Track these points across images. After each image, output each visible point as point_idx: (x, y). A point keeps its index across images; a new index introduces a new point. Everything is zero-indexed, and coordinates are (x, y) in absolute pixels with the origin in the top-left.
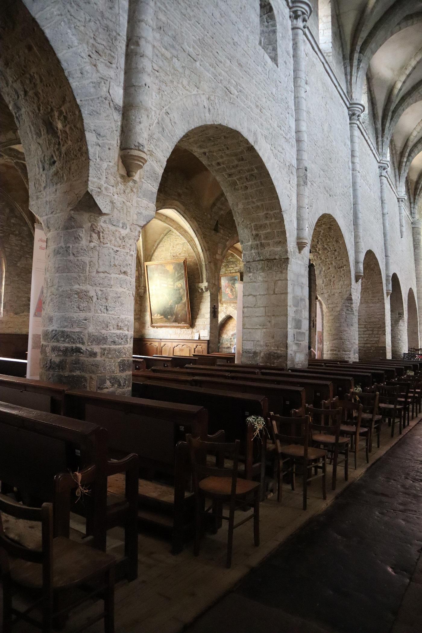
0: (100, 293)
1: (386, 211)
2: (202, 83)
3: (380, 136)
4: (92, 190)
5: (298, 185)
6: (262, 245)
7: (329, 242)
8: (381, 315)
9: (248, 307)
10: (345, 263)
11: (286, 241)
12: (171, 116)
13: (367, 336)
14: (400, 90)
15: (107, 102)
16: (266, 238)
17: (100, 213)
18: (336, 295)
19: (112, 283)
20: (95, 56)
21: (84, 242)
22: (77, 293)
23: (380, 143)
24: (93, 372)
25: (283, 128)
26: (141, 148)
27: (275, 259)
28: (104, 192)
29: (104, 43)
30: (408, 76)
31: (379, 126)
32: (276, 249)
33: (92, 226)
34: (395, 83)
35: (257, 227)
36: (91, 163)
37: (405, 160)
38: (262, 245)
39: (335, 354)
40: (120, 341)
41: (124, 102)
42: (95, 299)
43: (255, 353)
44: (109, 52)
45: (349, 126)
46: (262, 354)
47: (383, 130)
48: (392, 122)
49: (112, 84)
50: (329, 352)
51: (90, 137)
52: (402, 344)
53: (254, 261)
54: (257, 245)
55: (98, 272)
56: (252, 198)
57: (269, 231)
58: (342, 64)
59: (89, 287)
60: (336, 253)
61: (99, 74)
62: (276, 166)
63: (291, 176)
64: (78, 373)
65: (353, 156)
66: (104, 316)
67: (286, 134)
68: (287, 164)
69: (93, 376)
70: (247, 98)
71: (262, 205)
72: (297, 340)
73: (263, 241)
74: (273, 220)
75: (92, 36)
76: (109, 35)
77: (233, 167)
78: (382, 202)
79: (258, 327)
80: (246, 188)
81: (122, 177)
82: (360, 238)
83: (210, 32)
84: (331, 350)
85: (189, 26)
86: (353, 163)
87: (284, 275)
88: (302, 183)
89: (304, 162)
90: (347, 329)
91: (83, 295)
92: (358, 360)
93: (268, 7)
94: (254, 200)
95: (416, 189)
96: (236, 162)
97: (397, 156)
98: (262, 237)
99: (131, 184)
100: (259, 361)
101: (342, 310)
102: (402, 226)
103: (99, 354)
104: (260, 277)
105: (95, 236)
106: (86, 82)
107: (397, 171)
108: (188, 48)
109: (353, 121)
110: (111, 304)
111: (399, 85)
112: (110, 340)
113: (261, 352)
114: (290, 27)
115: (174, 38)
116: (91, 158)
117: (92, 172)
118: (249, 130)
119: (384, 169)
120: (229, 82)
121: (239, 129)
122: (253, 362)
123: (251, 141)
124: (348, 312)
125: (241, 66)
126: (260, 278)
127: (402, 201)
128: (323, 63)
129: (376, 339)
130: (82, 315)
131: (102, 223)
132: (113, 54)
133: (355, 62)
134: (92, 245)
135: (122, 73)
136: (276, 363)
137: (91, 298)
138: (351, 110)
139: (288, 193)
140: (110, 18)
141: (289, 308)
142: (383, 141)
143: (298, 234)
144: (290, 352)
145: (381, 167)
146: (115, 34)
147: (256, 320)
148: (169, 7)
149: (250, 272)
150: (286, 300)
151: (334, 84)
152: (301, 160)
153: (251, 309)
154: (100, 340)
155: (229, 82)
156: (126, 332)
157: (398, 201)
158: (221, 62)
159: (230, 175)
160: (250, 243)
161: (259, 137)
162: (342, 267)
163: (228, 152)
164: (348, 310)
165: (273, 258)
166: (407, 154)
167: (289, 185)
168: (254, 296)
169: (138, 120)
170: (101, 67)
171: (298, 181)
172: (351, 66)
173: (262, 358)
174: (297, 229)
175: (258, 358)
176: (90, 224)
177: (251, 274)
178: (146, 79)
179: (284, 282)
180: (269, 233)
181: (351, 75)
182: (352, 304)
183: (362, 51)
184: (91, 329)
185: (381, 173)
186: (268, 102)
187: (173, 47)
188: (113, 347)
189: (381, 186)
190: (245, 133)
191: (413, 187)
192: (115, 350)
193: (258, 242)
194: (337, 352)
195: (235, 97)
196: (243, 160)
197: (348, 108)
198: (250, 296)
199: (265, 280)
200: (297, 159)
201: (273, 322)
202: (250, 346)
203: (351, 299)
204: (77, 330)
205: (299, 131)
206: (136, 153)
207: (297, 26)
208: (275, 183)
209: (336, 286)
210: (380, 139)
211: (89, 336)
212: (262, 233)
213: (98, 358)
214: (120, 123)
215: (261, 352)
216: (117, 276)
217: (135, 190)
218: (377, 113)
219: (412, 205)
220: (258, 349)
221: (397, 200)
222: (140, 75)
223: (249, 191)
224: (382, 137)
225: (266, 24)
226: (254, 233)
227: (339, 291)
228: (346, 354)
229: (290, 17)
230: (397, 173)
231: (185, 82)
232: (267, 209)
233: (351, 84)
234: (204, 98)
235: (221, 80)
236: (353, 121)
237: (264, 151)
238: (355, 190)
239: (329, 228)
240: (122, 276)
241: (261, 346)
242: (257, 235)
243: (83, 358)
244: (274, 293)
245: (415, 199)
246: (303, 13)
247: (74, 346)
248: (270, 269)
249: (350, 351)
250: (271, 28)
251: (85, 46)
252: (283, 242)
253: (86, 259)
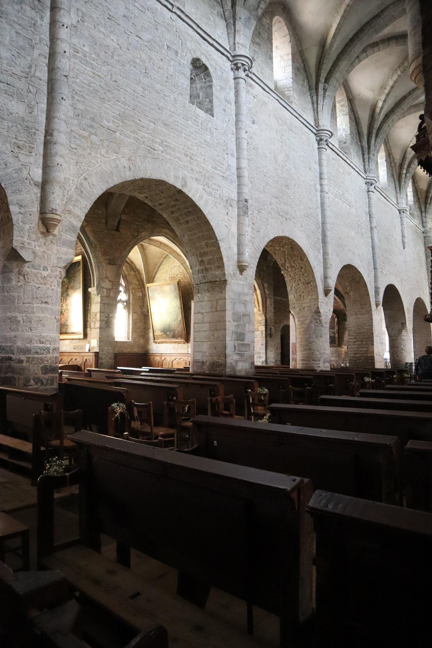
0: (25, 318)
1: (374, 225)
2: (121, 148)
3: (366, 153)
4: (16, 246)
5: (239, 216)
6: (206, 270)
7: (294, 261)
8: (369, 325)
9: (197, 323)
10: (311, 279)
11: (224, 265)
12: (89, 180)
13: (357, 346)
14: (382, 108)
15: (28, 181)
16: (209, 263)
17: (24, 261)
18: (306, 308)
19: (35, 310)
20: (16, 150)
21: (14, 283)
22: (10, 319)
23: (366, 160)
24: (20, 374)
25: (219, 168)
26: (54, 212)
27: (216, 281)
28: (27, 246)
29: (24, 139)
30: (388, 95)
31: (365, 144)
33: (19, 271)
34: (377, 102)
35: (202, 255)
36: (15, 227)
37: (405, 171)
38: (206, 270)
39: (306, 364)
40: (42, 352)
41: (43, 179)
42: (22, 322)
44: (29, 144)
45: (317, 151)
46: (208, 363)
47: (369, 147)
48: (378, 139)
49: (31, 167)
50: (301, 362)
51: (13, 209)
52: (406, 353)
53: (201, 283)
55: (24, 303)
57: (210, 257)
58: (309, 94)
59: (17, 314)
60: (303, 271)
61: (20, 163)
62: (210, 202)
63: (230, 208)
64: (9, 375)
65: (321, 178)
66: (29, 334)
67: (224, 173)
68: (225, 199)
69: (21, 377)
70: (174, 150)
71: (202, 235)
72: (239, 351)
73: (207, 266)
74: (212, 248)
75: (14, 136)
76: (29, 133)
77: (172, 206)
78: (370, 216)
79: (205, 340)
80: (187, 222)
81: (42, 233)
82: (328, 255)
83: (131, 105)
84: (303, 360)
85: (108, 106)
86: (321, 185)
87: (223, 295)
88: (242, 213)
89: (244, 195)
90: (315, 340)
91: (14, 320)
92: (329, 369)
93: (204, 67)
94: (196, 232)
95: (427, 198)
96: (173, 203)
97: (397, 168)
99: (51, 237)
100: (206, 369)
101: (311, 322)
102: (404, 237)
103: (25, 361)
104: (206, 296)
105: (21, 278)
106: (9, 171)
107: (397, 183)
108: (107, 124)
109: (321, 146)
110: (34, 325)
111: (380, 104)
112: (33, 351)
113: (207, 361)
114: (233, 77)
115: (93, 119)
116: (14, 223)
117: (15, 233)
118: (176, 177)
119: (371, 185)
120: (153, 141)
121: (164, 178)
122: (202, 371)
123: (179, 186)
124: (317, 324)
125: (168, 125)
126: (206, 298)
127: (404, 212)
128: (277, 100)
129: (365, 349)
130: (13, 334)
131: (26, 268)
132: (32, 145)
133: (321, 92)
134: (19, 284)
135: (41, 158)
136: (218, 371)
137: (19, 322)
138: (318, 136)
139: (226, 224)
140: (30, 120)
141: (227, 323)
142: (369, 158)
143: (238, 258)
144: (229, 360)
145: (368, 182)
146: (34, 130)
147: (203, 334)
148: (87, 97)
149: (199, 293)
150: (224, 316)
151: (295, 116)
152: (241, 193)
154: (27, 351)
155: (153, 141)
156: (49, 346)
157: (400, 213)
158: (144, 127)
159: (172, 213)
160: (197, 268)
161: (189, 181)
162: (309, 283)
163: (163, 195)
164: (316, 322)
165: (215, 280)
166: (406, 166)
167: (227, 217)
168: (202, 313)
169: (51, 191)
170: (21, 157)
171: (238, 212)
172: (317, 95)
173: (208, 366)
174: (238, 254)
176: (17, 270)
177: (200, 295)
178: (58, 160)
179: (223, 300)
180: (210, 259)
181: (317, 104)
182: (320, 316)
183: (327, 81)
184: (19, 344)
185: (368, 189)
186: (200, 149)
187: (92, 126)
188: (36, 356)
189: (369, 201)
190: (171, 180)
191: (424, 196)
192: (38, 358)
193: (203, 267)
194: (307, 362)
195: (159, 152)
196: (177, 200)
197: (315, 134)
198: (199, 314)
200: (238, 193)
201: (216, 335)
202: (199, 357)
203: (319, 312)
204: (10, 344)
205: (239, 168)
206: (50, 216)
207: (238, 76)
208: (209, 217)
209: (306, 301)
210: (366, 156)
211: (18, 348)
212: (206, 259)
213: (24, 364)
214: (39, 195)
215: (207, 361)
216: (39, 305)
217: (54, 242)
218: (362, 132)
219: (424, 214)
220: (205, 359)
221: (398, 212)
222: (53, 158)
224: (369, 154)
225: (204, 80)
226: (200, 259)
227: (308, 305)
228: (316, 364)
229: (232, 69)
230: (397, 186)
231: (103, 151)
232: (207, 239)
233: (317, 113)
234: (123, 160)
235: (144, 142)
236: (321, 146)
237: (196, 193)
238: (323, 210)
239: (292, 248)
240: (43, 305)
241: (207, 356)
242: (202, 261)
243: (13, 364)
244: (216, 311)
245: (426, 208)
246: (243, 65)
247: (7, 355)
248: (213, 290)
249: (319, 361)
250: (208, 84)
251: (8, 145)
252: (221, 266)
253: (15, 294)
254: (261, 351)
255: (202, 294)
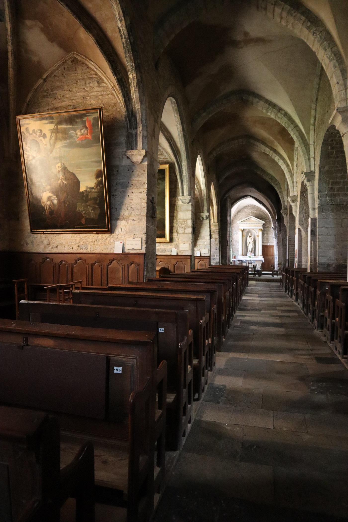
6: (335, 195)
9: (322, 235)
16: (338, 190)
27: (343, 204)
32: (344, 198)
43: (329, 265)
46: (334, 266)
54: (331, 195)
56: (338, 164)
80: (337, 157)
94: (338, 166)
98: (336, 190)
113: (332, 264)
122: (327, 271)
126: (331, 216)
147: (328, 243)
149: (323, 212)
153: (324, 236)
160: (326, 193)
168: (327, 228)
173: (334, 268)
175: (331, 268)
177: (324, 213)
193: (332, 193)
199: (335, 217)
202: (324, 260)
212: (336, 187)
220: (331, 262)
223: (339, 159)
226: (330, 186)
241: (333, 260)
242: (332, 188)
244: (342, 227)
254: (215, 254)
255: (325, 213)
